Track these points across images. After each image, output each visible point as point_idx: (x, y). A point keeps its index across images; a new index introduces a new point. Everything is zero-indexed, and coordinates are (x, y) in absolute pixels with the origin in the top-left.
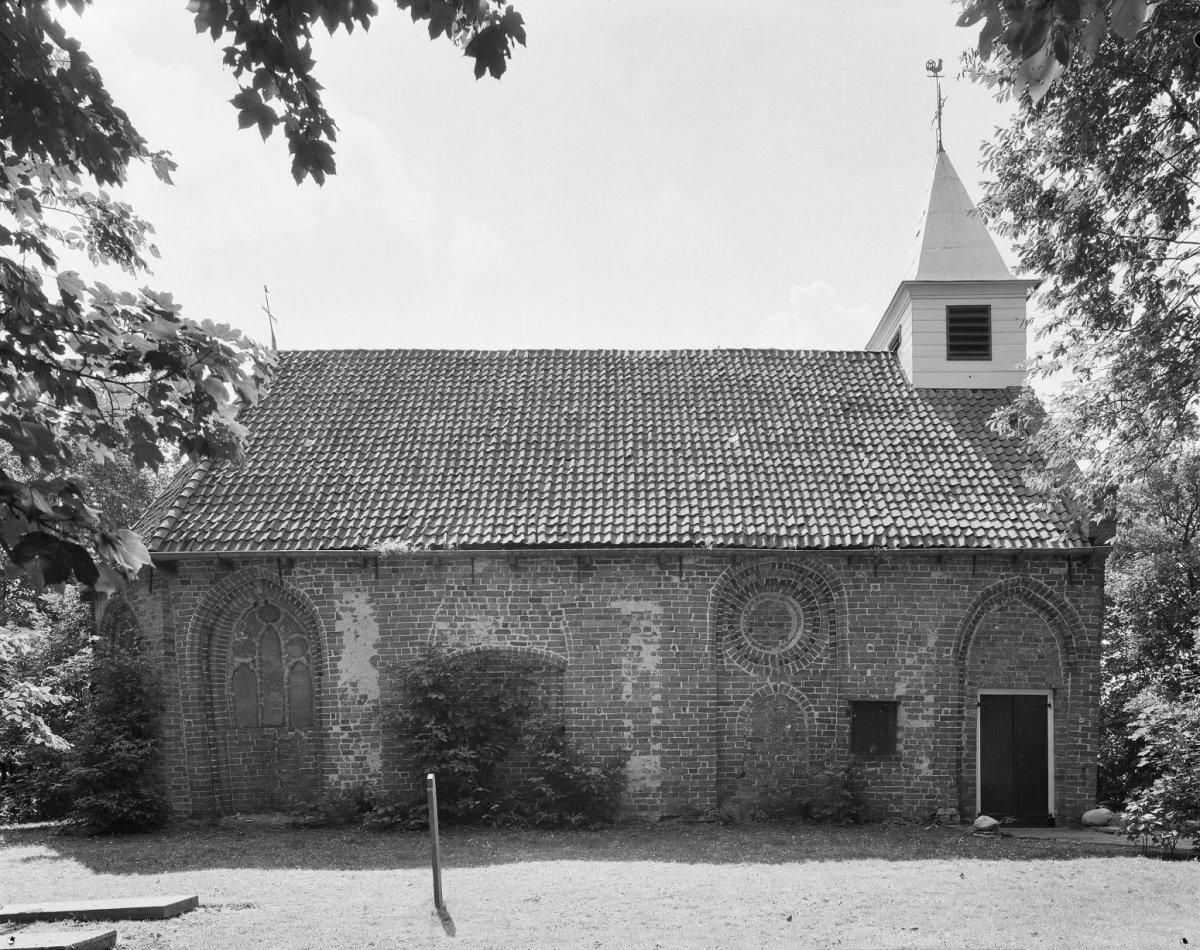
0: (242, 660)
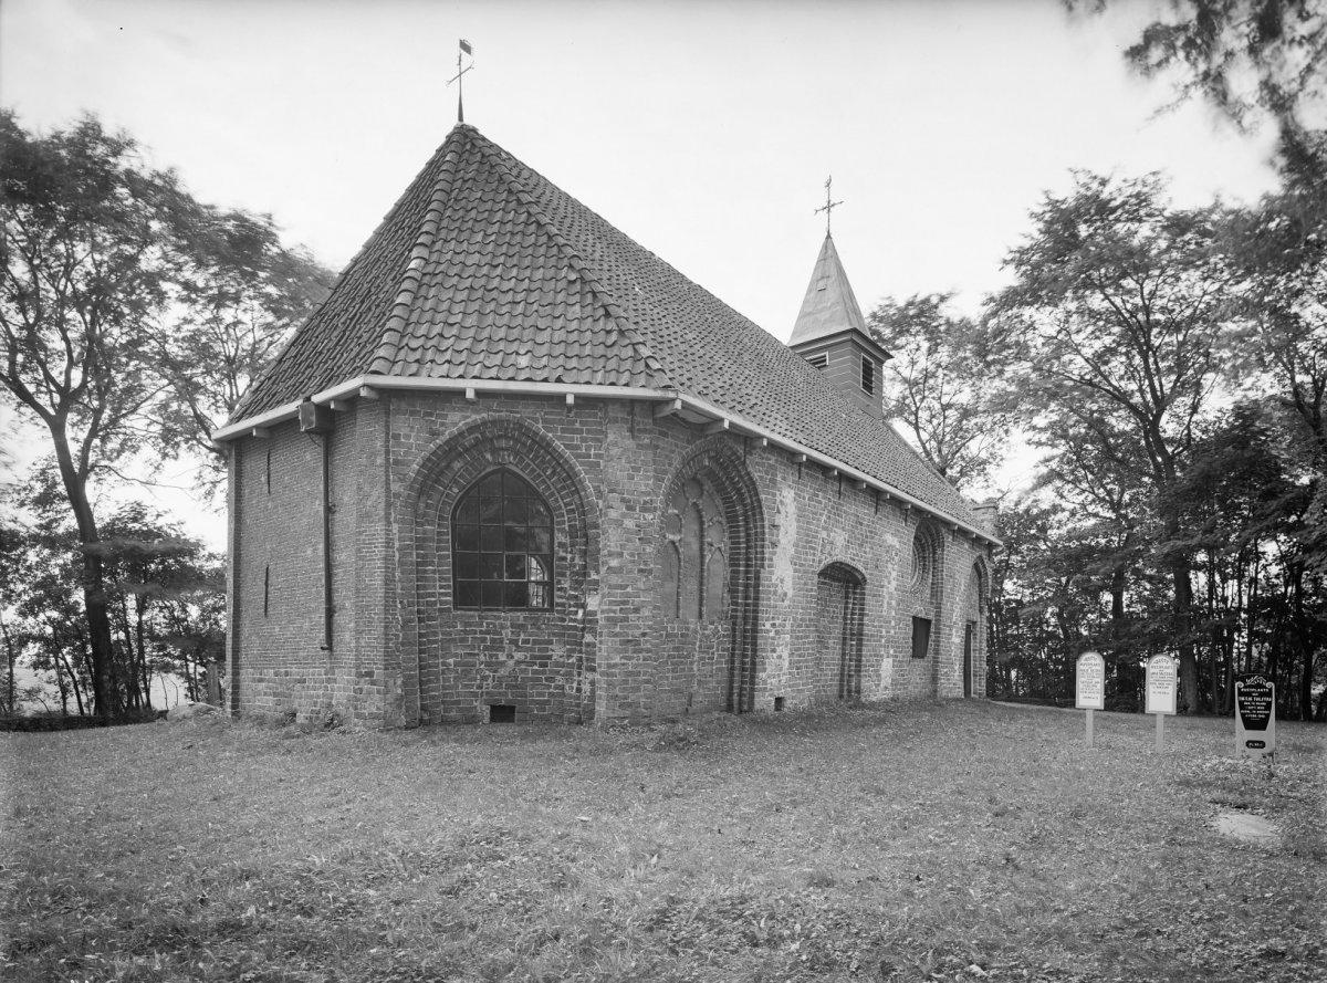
0: (671, 537)
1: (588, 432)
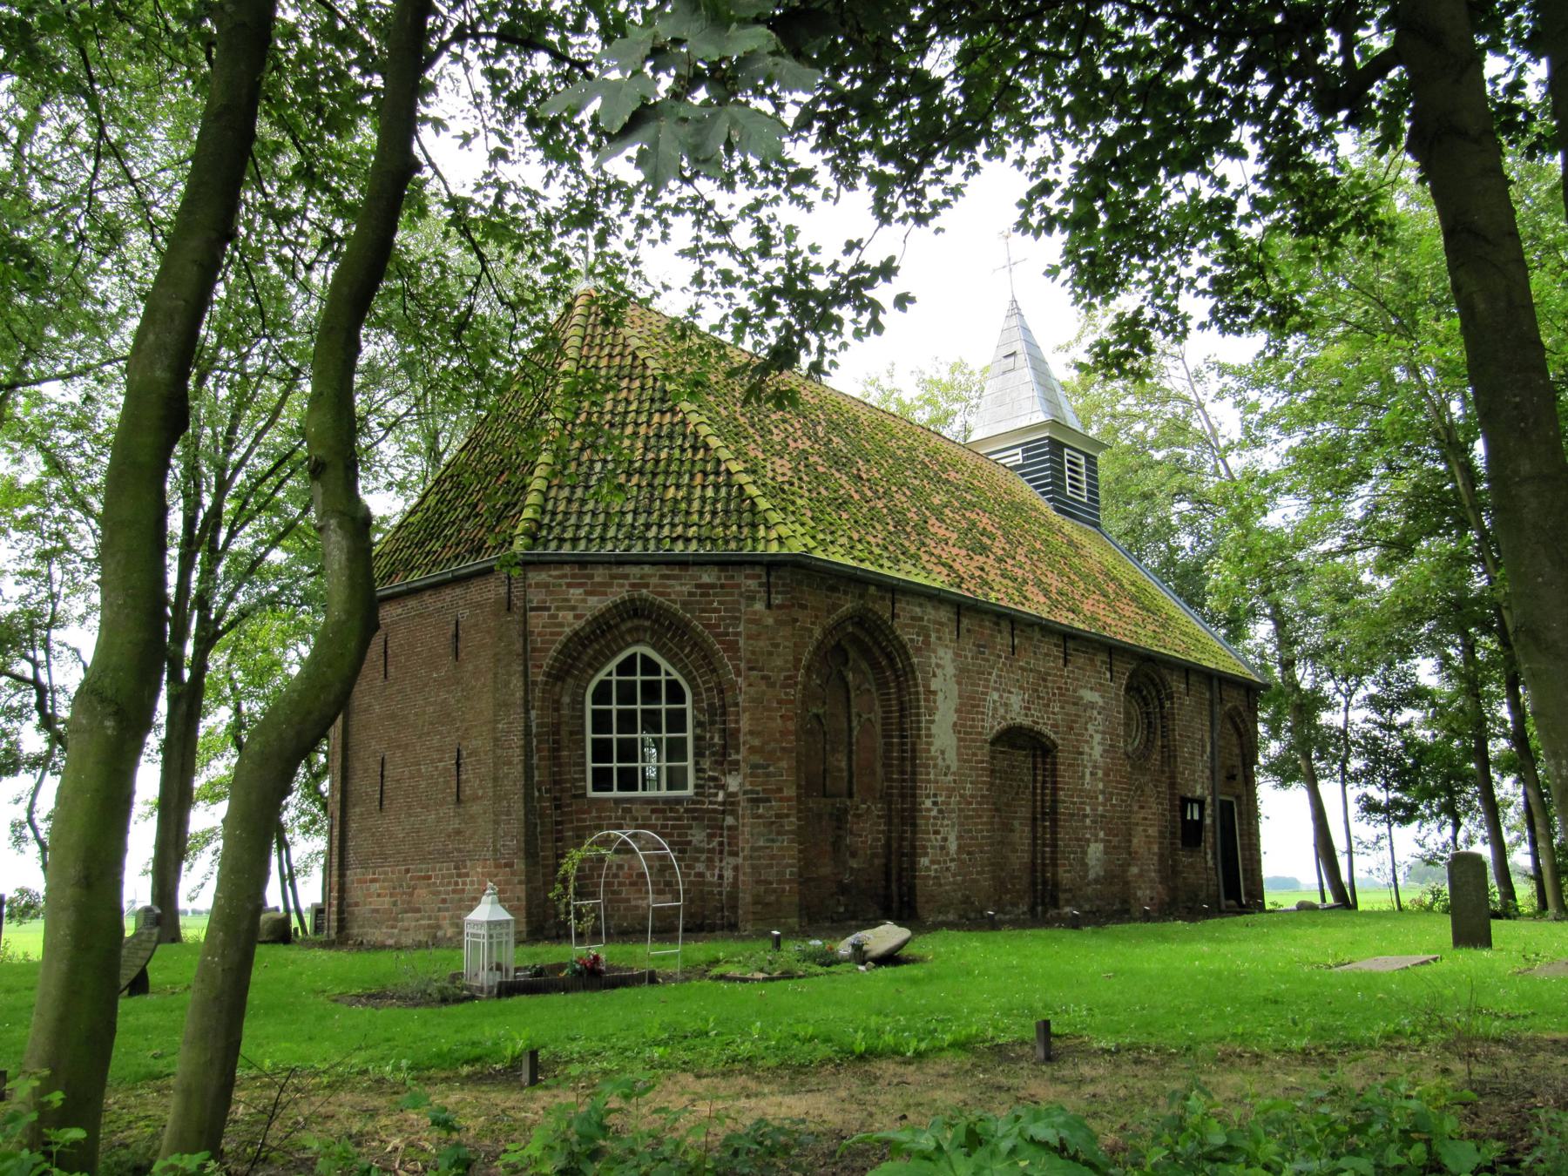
1: (726, 610)
